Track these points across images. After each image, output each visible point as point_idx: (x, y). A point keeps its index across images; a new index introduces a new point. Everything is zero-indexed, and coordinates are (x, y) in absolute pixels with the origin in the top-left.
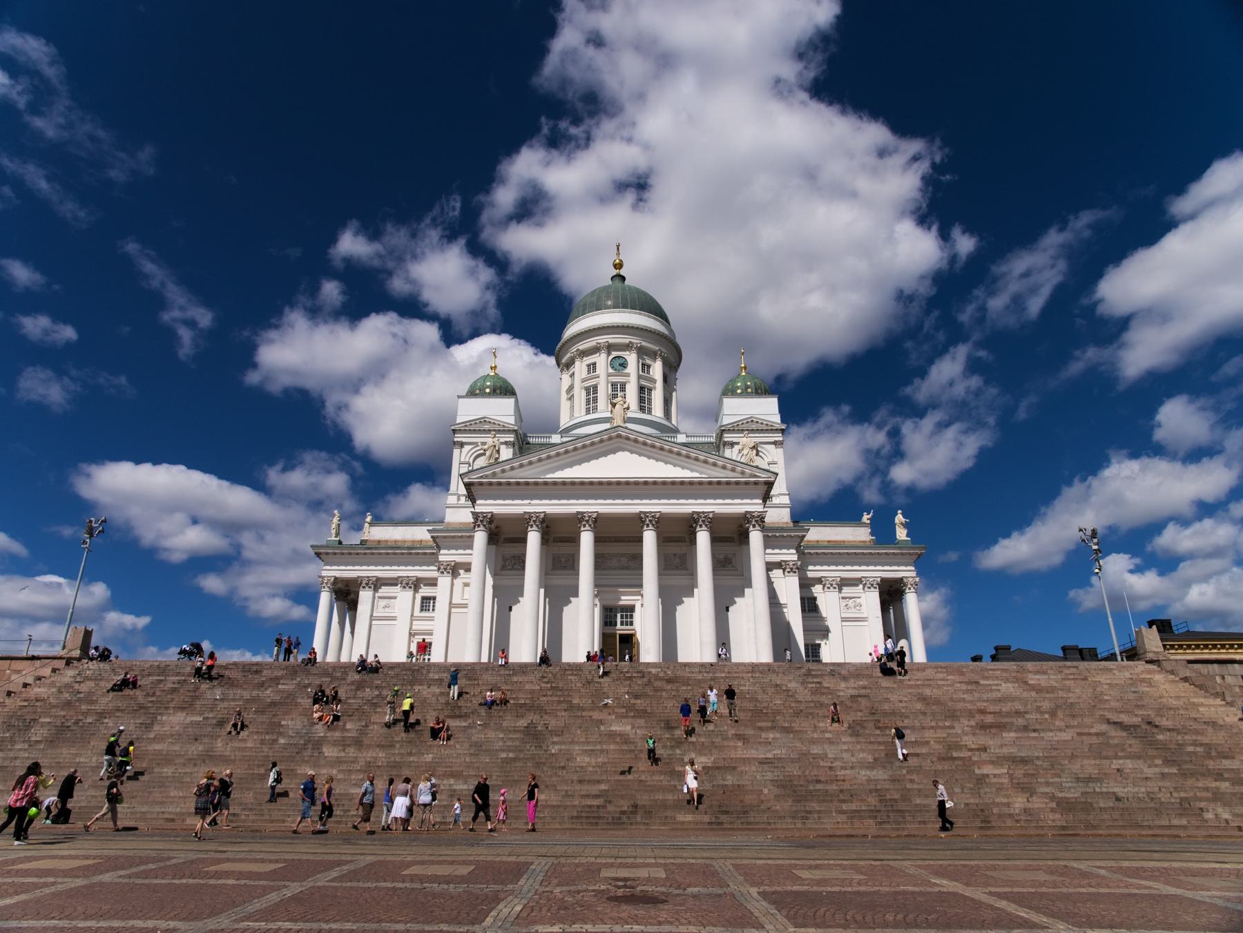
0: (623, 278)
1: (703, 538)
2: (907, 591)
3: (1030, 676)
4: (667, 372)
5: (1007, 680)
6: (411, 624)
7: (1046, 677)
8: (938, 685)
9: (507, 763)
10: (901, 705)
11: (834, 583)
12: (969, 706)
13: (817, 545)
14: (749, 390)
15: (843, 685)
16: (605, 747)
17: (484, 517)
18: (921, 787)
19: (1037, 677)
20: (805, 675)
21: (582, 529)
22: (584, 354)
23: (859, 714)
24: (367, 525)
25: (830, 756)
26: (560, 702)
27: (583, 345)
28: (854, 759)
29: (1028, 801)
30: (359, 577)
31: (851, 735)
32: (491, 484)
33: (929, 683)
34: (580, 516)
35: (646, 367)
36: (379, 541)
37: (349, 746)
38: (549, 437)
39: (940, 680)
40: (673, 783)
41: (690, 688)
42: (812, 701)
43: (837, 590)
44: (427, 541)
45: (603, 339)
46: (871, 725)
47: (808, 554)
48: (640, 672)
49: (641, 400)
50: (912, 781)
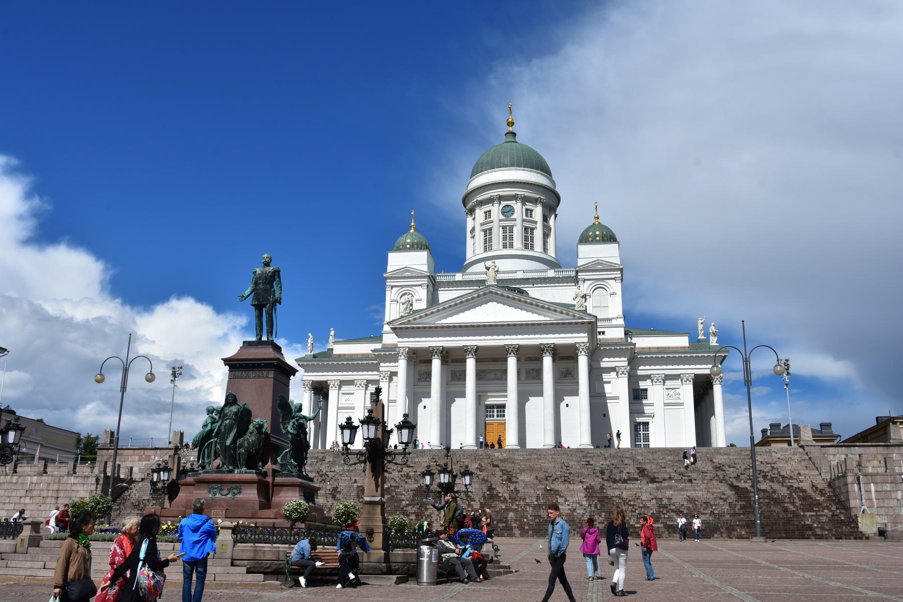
0: (514, 134)
4: (547, 213)
11: (660, 378)
13: (649, 350)
14: (598, 238)
24: (331, 337)
27: (481, 197)
34: (465, 348)
35: (529, 212)
36: (340, 355)
38: (454, 276)
41: (513, 465)
43: (662, 383)
45: (495, 193)
47: (635, 359)
49: (526, 238)
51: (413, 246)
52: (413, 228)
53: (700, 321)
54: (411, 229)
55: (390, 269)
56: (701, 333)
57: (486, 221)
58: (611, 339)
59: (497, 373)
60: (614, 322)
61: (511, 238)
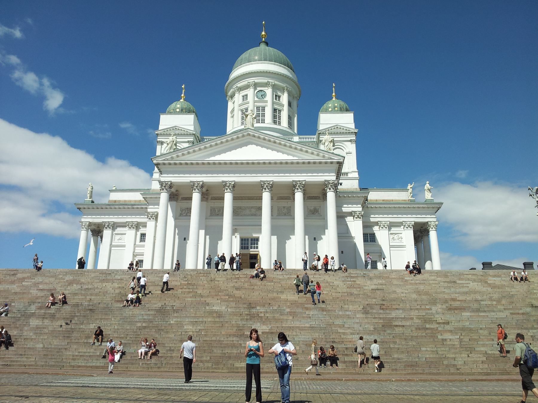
1: (299, 196)
2: (431, 229)
3: (490, 278)
4: (291, 101)
5: (474, 281)
6: (134, 249)
7: (500, 279)
8: (430, 283)
9: (140, 329)
10: (402, 295)
11: (386, 225)
12: (446, 296)
13: (376, 202)
14: (336, 109)
15: (369, 282)
16: (205, 319)
17: (166, 184)
18: (400, 346)
19: (494, 279)
20: (346, 276)
21: (226, 191)
22: (240, 89)
23: (374, 300)
25: (346, 326)
26: (190, 292)
27: (240, 84)
28: (361, 329)
29: (468, 356)
30: (103, 222)
31: (363, 313)
32: (170, 164)
33: (424, 282)
35: (278, 97)
36: (115, 201)
37: (46, 318)
39: (432, 280)
40: (240, 342)
41: (273, 284)
42: (347, 292)
43: (387, 229)
44: (143, 201)
46: (378, 307)
48: (245, 275)
49: (274, 117)
50: (395, 343)
51: (182, 110)
52: (183, 99)
53: (409, 186)
54: (181, 99)
55: (161, 128)
56: (411, 195)
57: (244, 102)
58: (348, 189)
59: (252, 209)
60: (350, 175)
61: (263, 115)
